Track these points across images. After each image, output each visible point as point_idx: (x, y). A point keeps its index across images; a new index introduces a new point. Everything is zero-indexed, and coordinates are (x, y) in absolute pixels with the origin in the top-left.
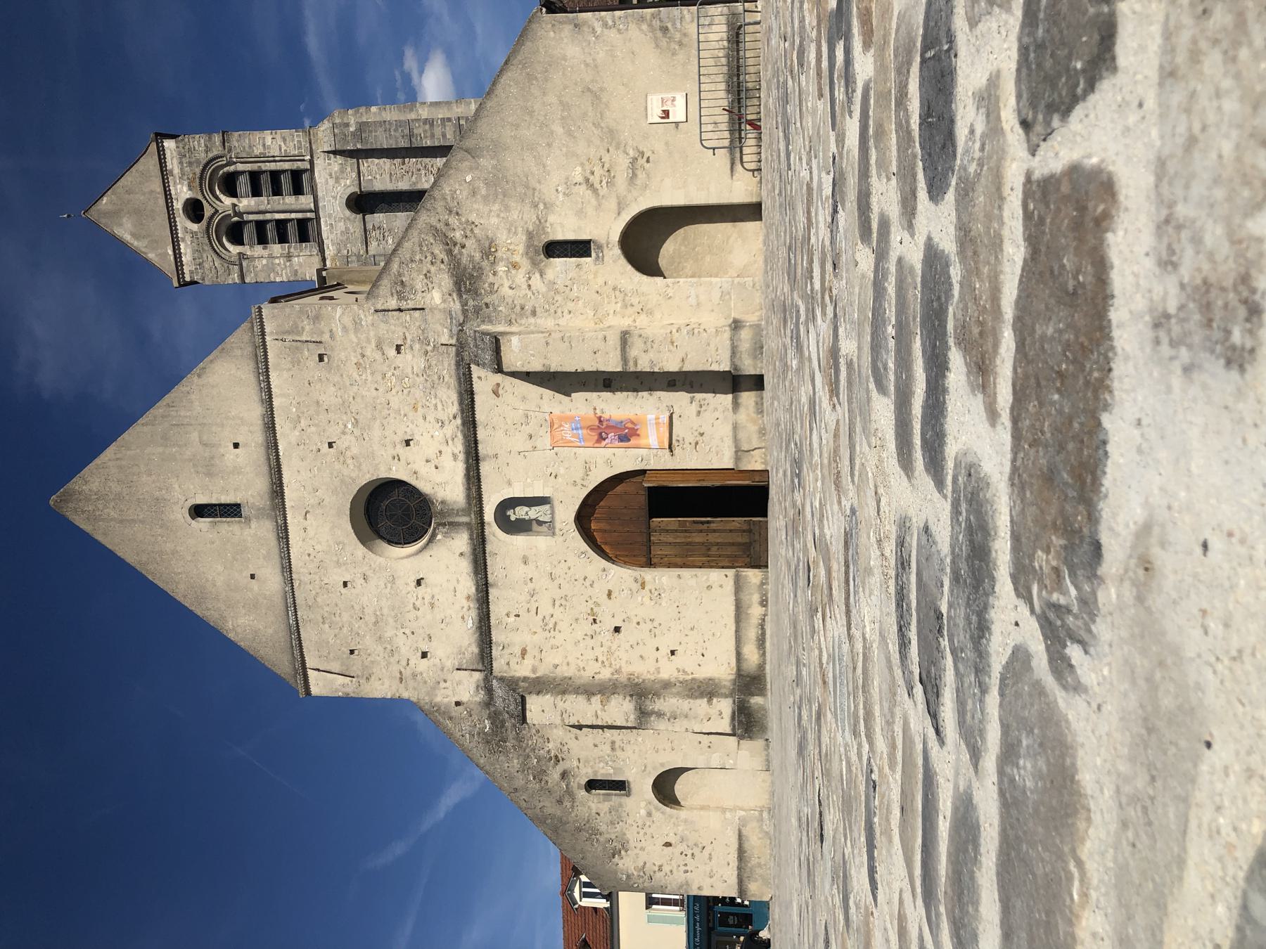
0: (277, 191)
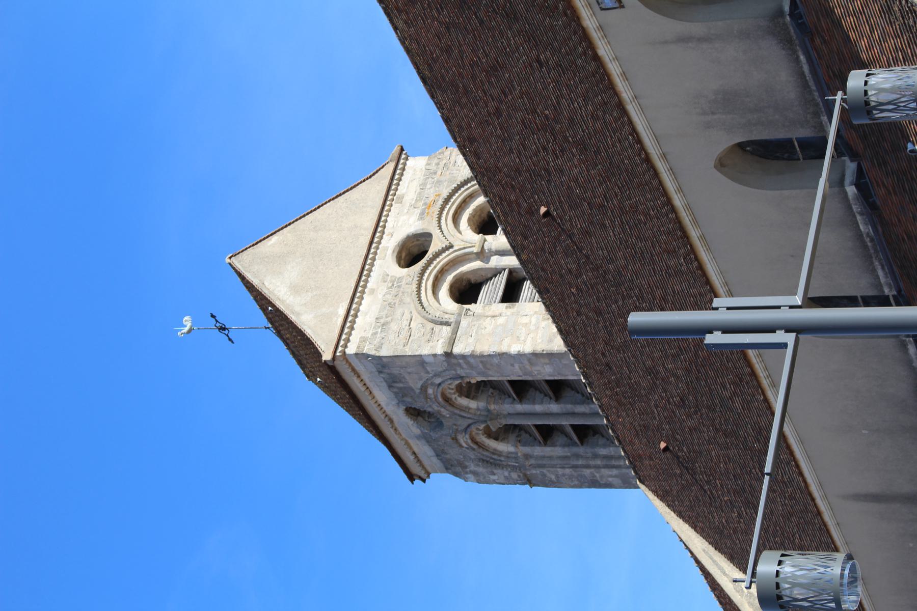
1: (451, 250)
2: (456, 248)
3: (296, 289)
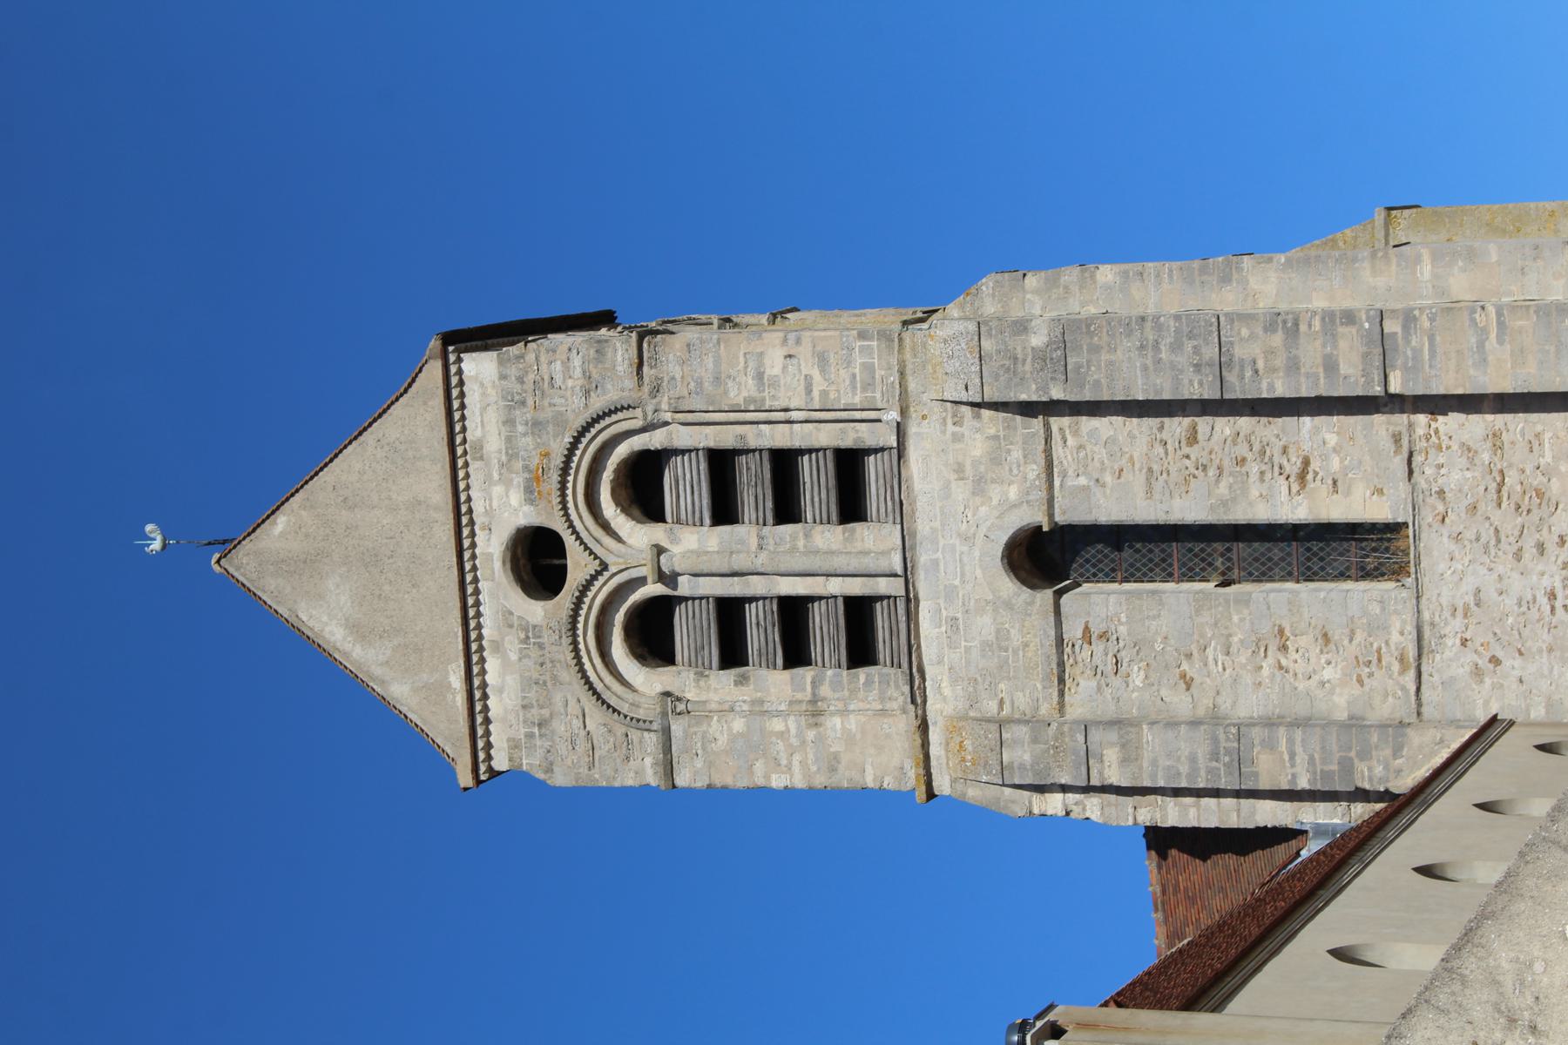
0: (787, 510)
1: (606, 574)
2: (613, 569)
3: (357, 629)
